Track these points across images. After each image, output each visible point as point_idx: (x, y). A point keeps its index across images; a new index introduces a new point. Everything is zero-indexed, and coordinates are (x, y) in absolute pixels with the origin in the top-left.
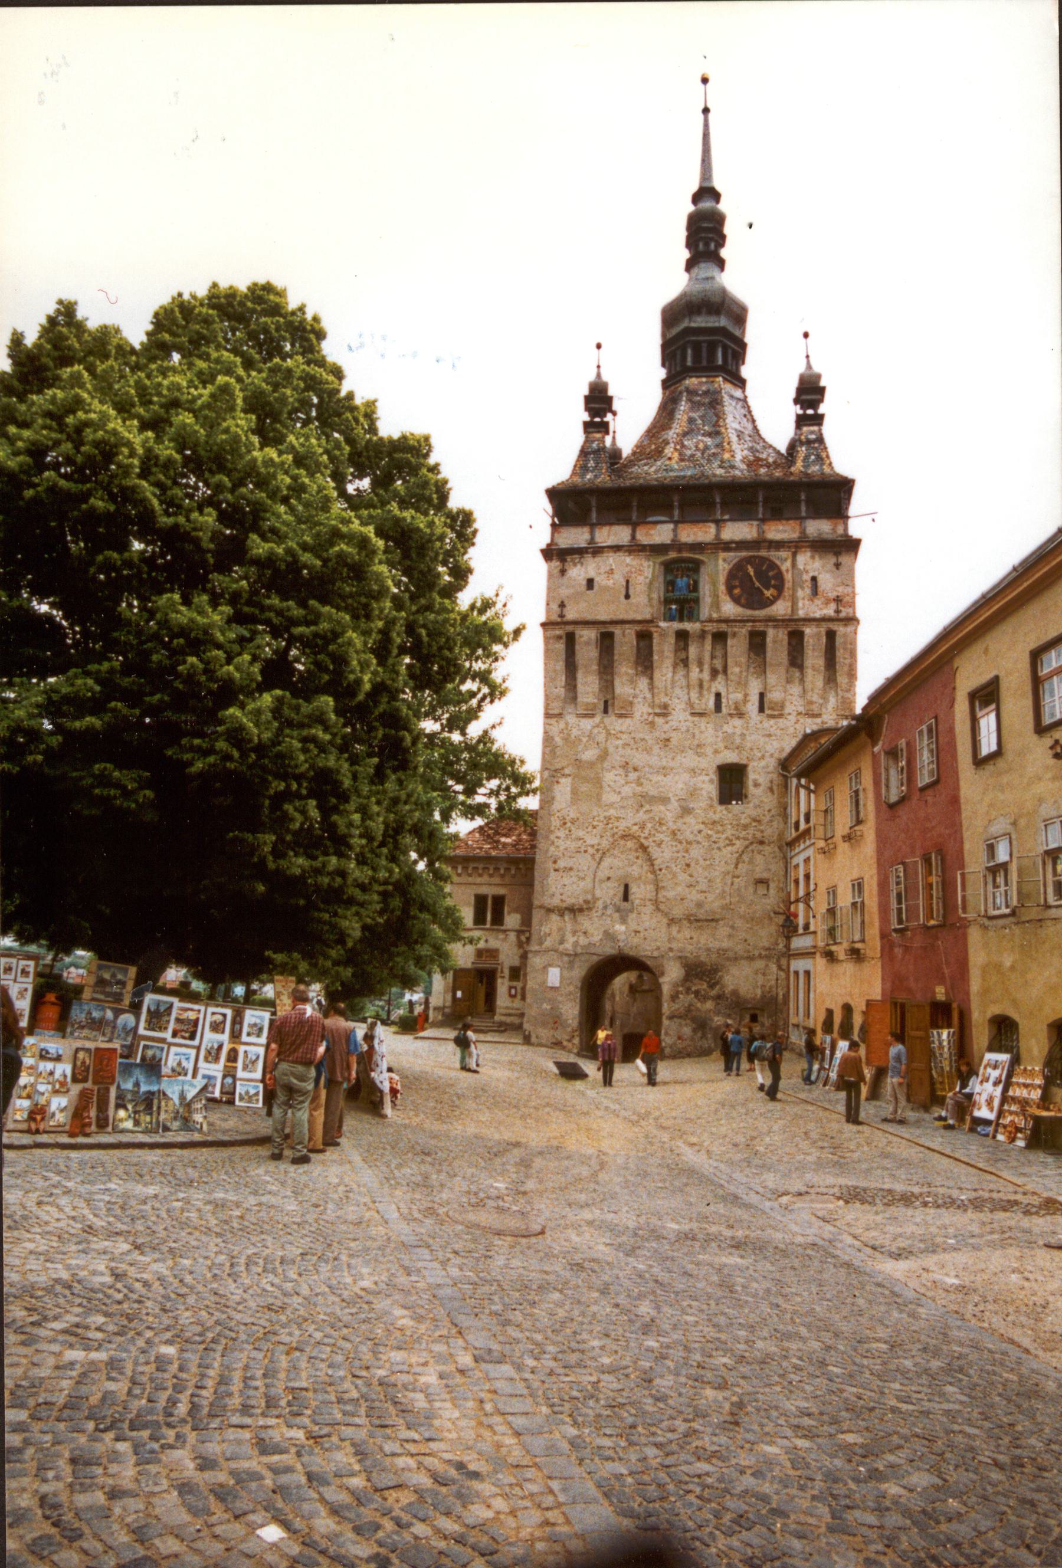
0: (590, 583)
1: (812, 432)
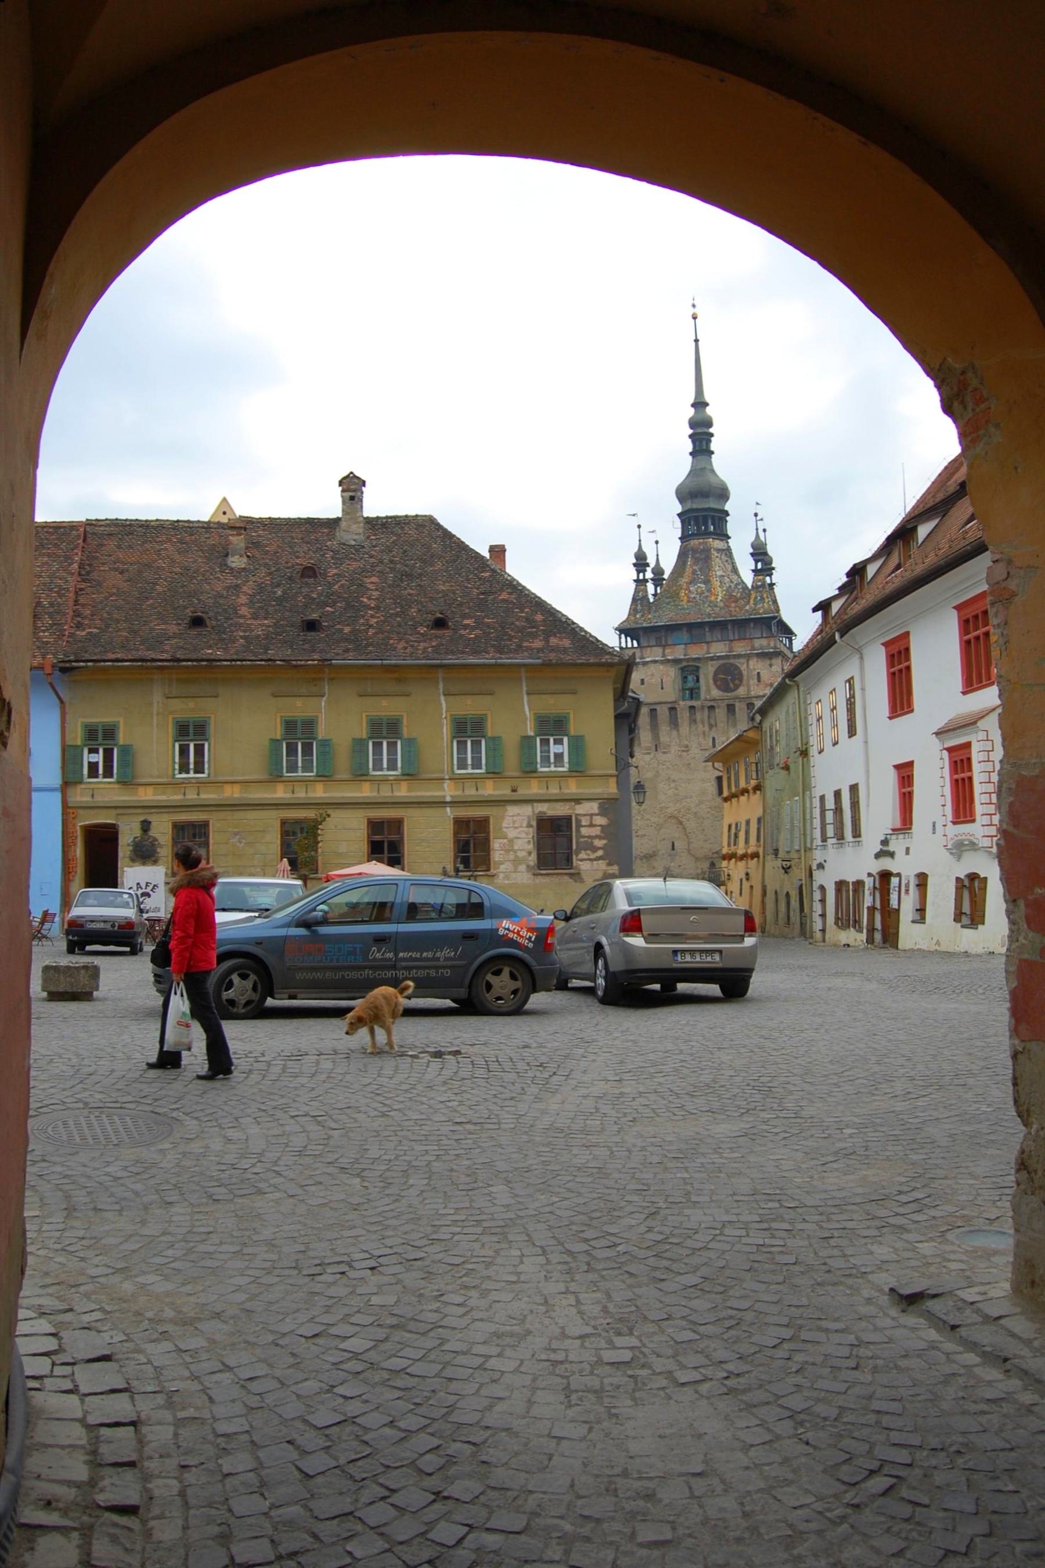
0: (642, 681)
1: (760, 581)
